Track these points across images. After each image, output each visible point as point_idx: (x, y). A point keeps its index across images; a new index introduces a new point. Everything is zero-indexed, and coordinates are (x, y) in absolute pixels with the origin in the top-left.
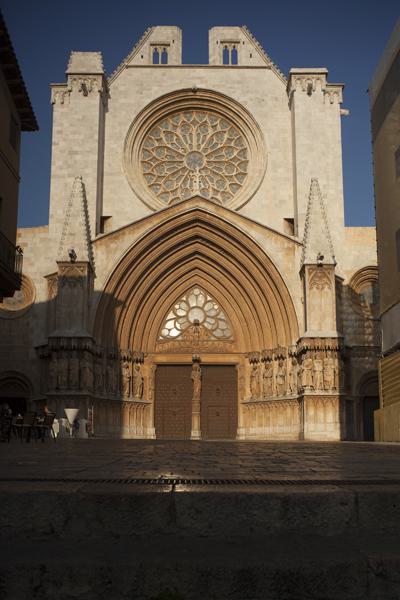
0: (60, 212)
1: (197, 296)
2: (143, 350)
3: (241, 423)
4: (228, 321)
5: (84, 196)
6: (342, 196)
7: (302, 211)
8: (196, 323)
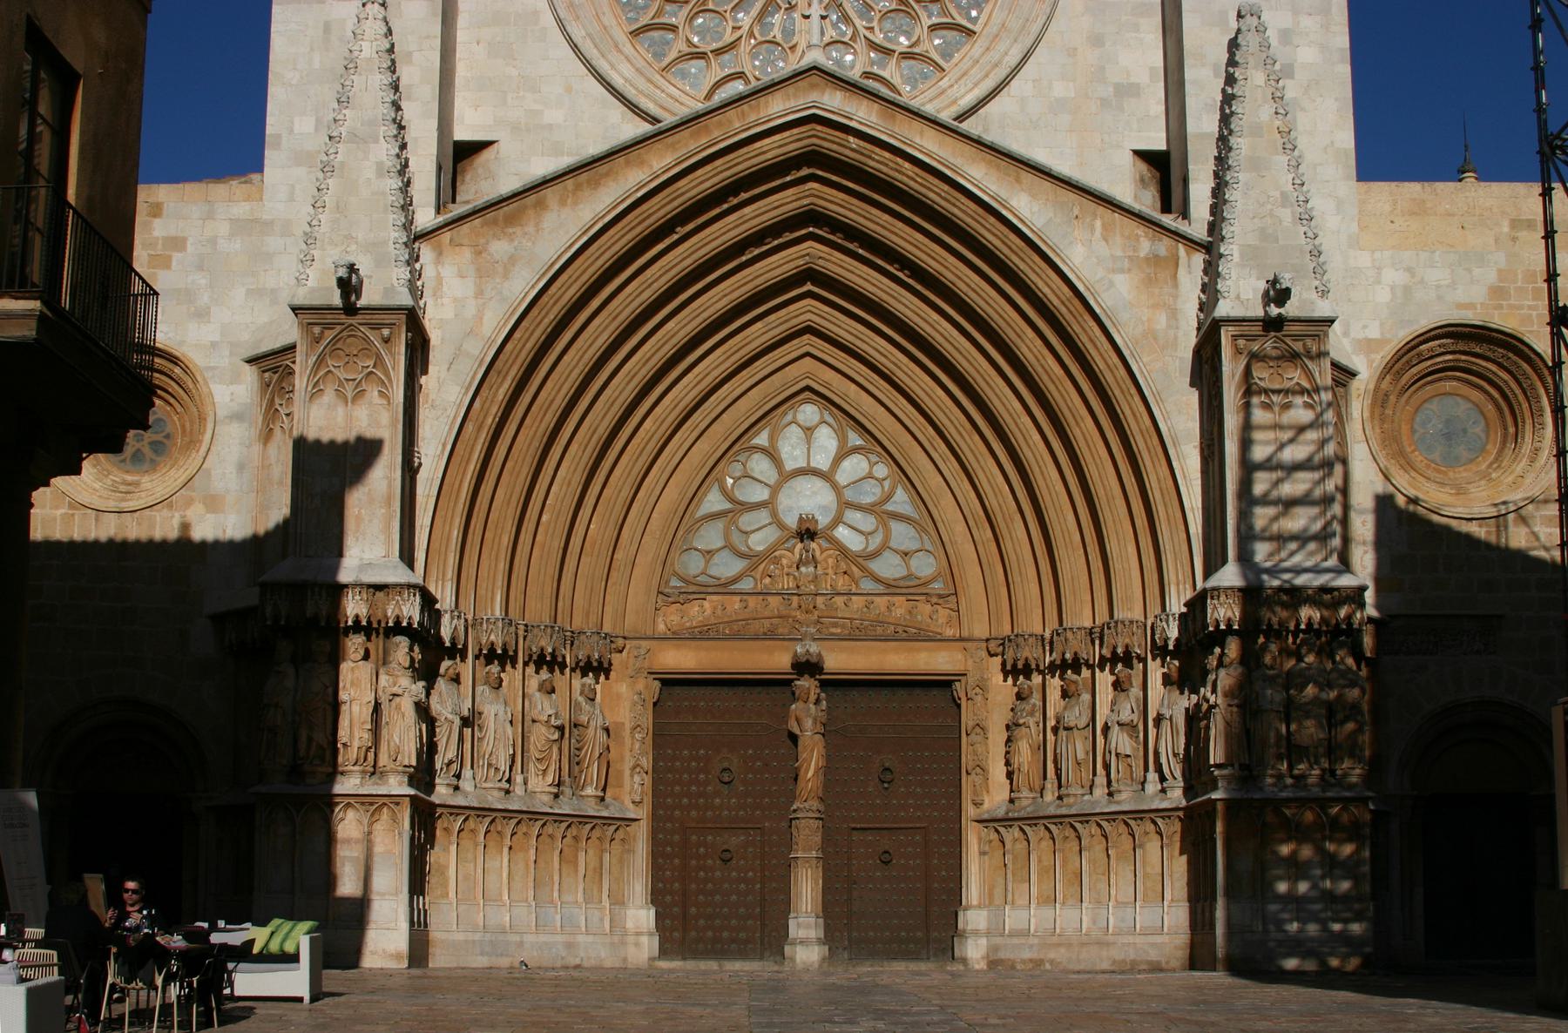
0: (305, 125)
1: (809, 431)
2: (607, 628)
3: (973, 889)
4: (927, 520)
5: (393, 68)
6: (1345, 70)
7: (1202, 123)
8: (807, 533)
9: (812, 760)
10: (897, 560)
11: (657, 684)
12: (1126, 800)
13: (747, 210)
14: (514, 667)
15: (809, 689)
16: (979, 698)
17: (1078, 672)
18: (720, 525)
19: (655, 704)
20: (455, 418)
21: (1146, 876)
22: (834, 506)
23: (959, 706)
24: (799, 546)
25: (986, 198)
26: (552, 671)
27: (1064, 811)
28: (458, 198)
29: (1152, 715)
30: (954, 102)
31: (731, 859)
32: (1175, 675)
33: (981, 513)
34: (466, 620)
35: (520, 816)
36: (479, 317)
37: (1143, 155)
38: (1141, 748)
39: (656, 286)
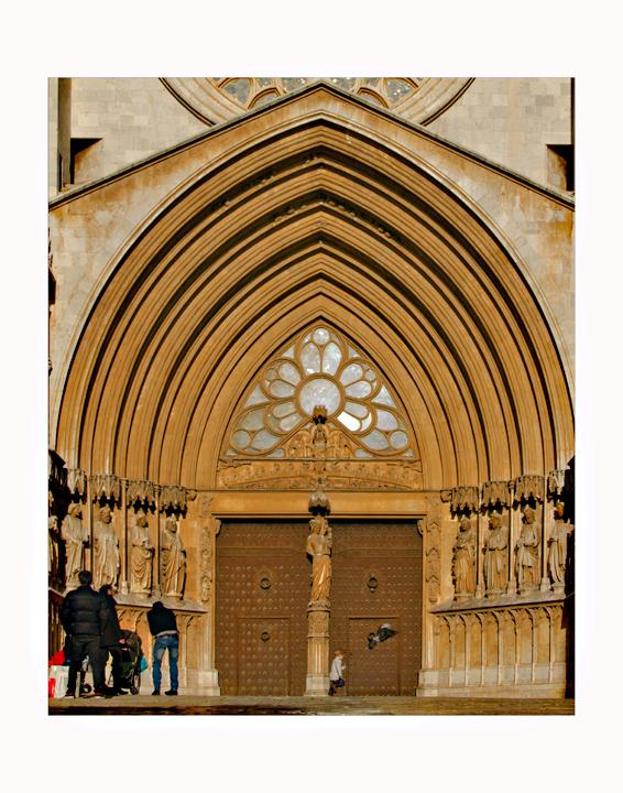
1: (322, 348)
2: (183, 484)
3: (429, 656)
4: (402, 410)
8: (320, 419)
9: (322, 573)
10: (381, 436)
11: (219, 522)
12: (528, 597)
13: (276, 189)
14: (119, 508)
15: (320, 525)
16: (435, 530)
17: (500, 512)
18: (260, 413)
19: (217, 536)
20: (75, 336)
21: (539, 646)
22: (339, 400)
23: (421, 536)
24: (315, 427)
25: (440, 180)
26: (146, 512)
27: (487, 605)
28: (75, 181)
29: (546, 539)
30: (423, 110)
31: (268, 639)
32: (561, 512)
33: (438, 403)
34: (85, 477)
35: (125, 608)
36: (89, 265)
37: (553, 148)
38: (540, 561)
39: (212, 244)
